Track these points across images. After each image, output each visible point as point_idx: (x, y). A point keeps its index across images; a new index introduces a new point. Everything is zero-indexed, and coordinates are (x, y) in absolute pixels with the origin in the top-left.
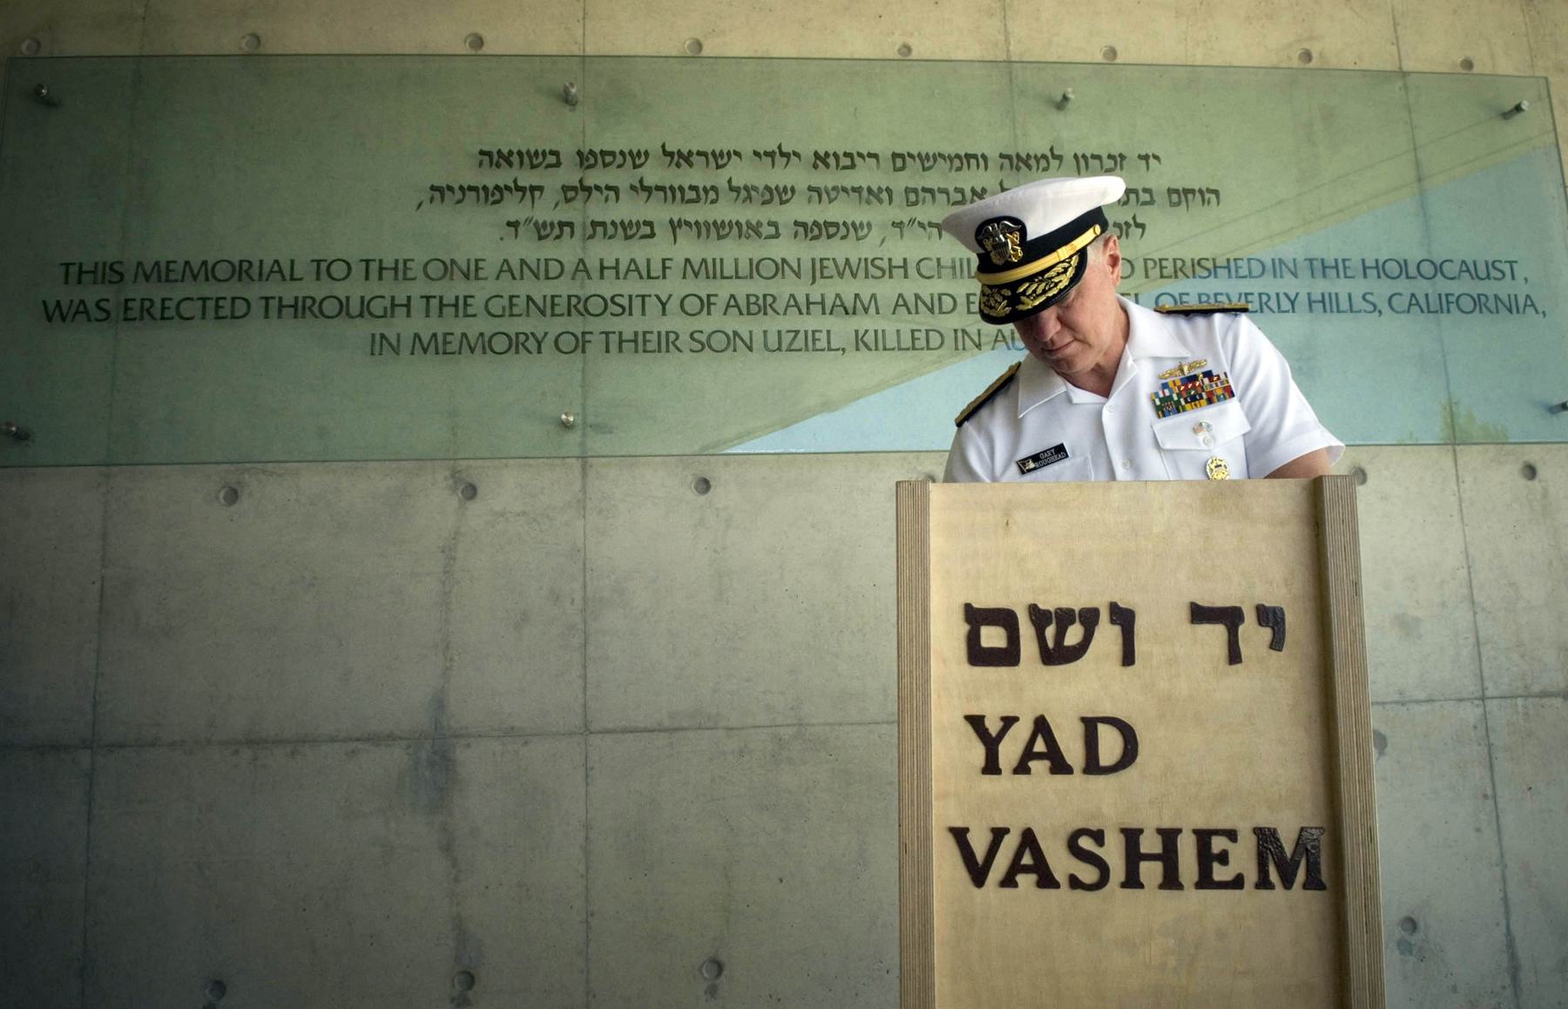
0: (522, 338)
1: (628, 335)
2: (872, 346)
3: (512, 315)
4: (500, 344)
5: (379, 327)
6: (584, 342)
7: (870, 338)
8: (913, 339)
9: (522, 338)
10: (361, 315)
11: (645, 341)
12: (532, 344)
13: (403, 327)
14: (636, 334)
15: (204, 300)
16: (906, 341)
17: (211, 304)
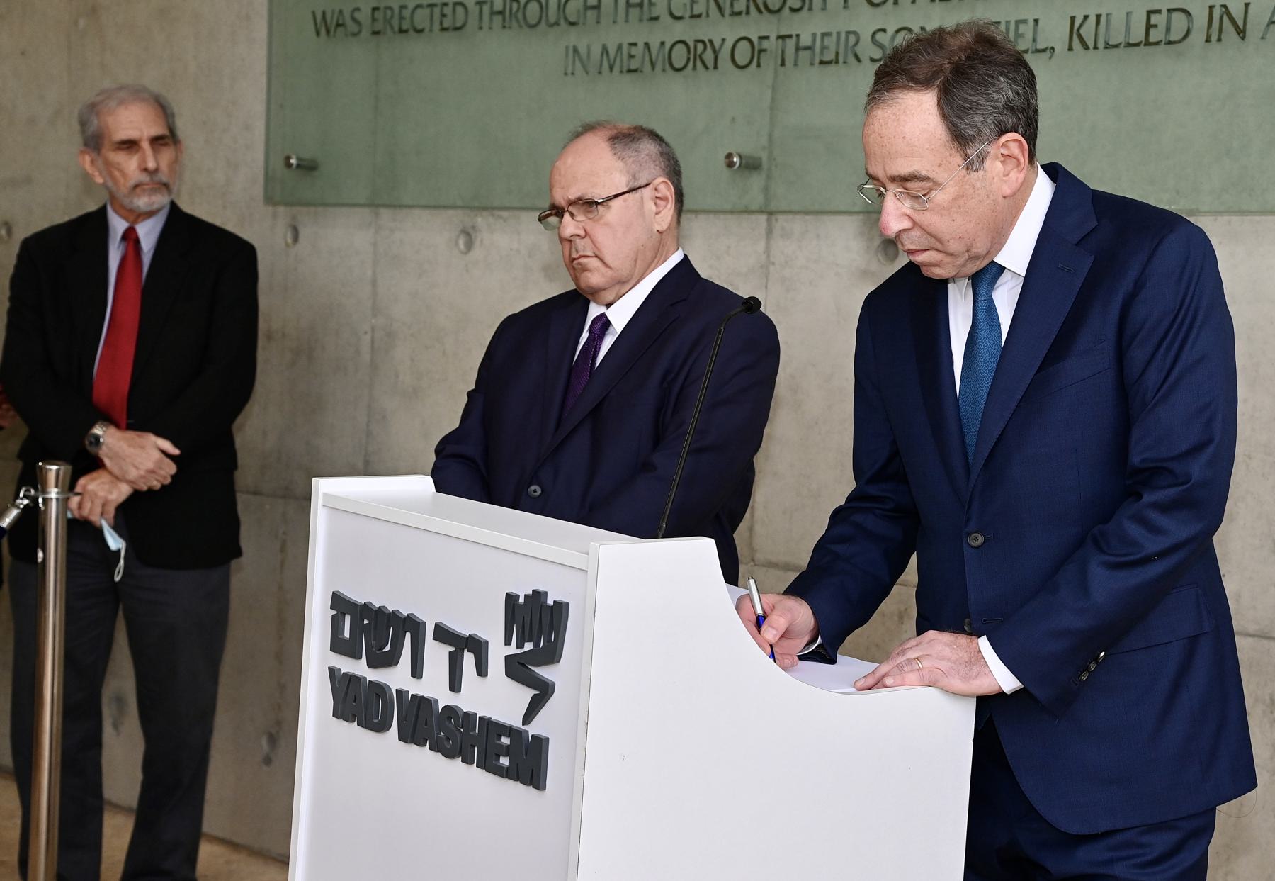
0: (700, 47)
1: (806, 40)
2: (1091, 44)
3: (693, 16)
4: (680, 55)
5: (573, 38)
6: (761, 51)
7: (1088, 31)
8: (1149, 26)
9: (700, 47)
10: (557, 23)
11: (823, 48)
12: (709, 56)
13: (590, 40)
14: (814, 35)
15: (431, 6)
16: (1138, 34)
17: (437, 11)
